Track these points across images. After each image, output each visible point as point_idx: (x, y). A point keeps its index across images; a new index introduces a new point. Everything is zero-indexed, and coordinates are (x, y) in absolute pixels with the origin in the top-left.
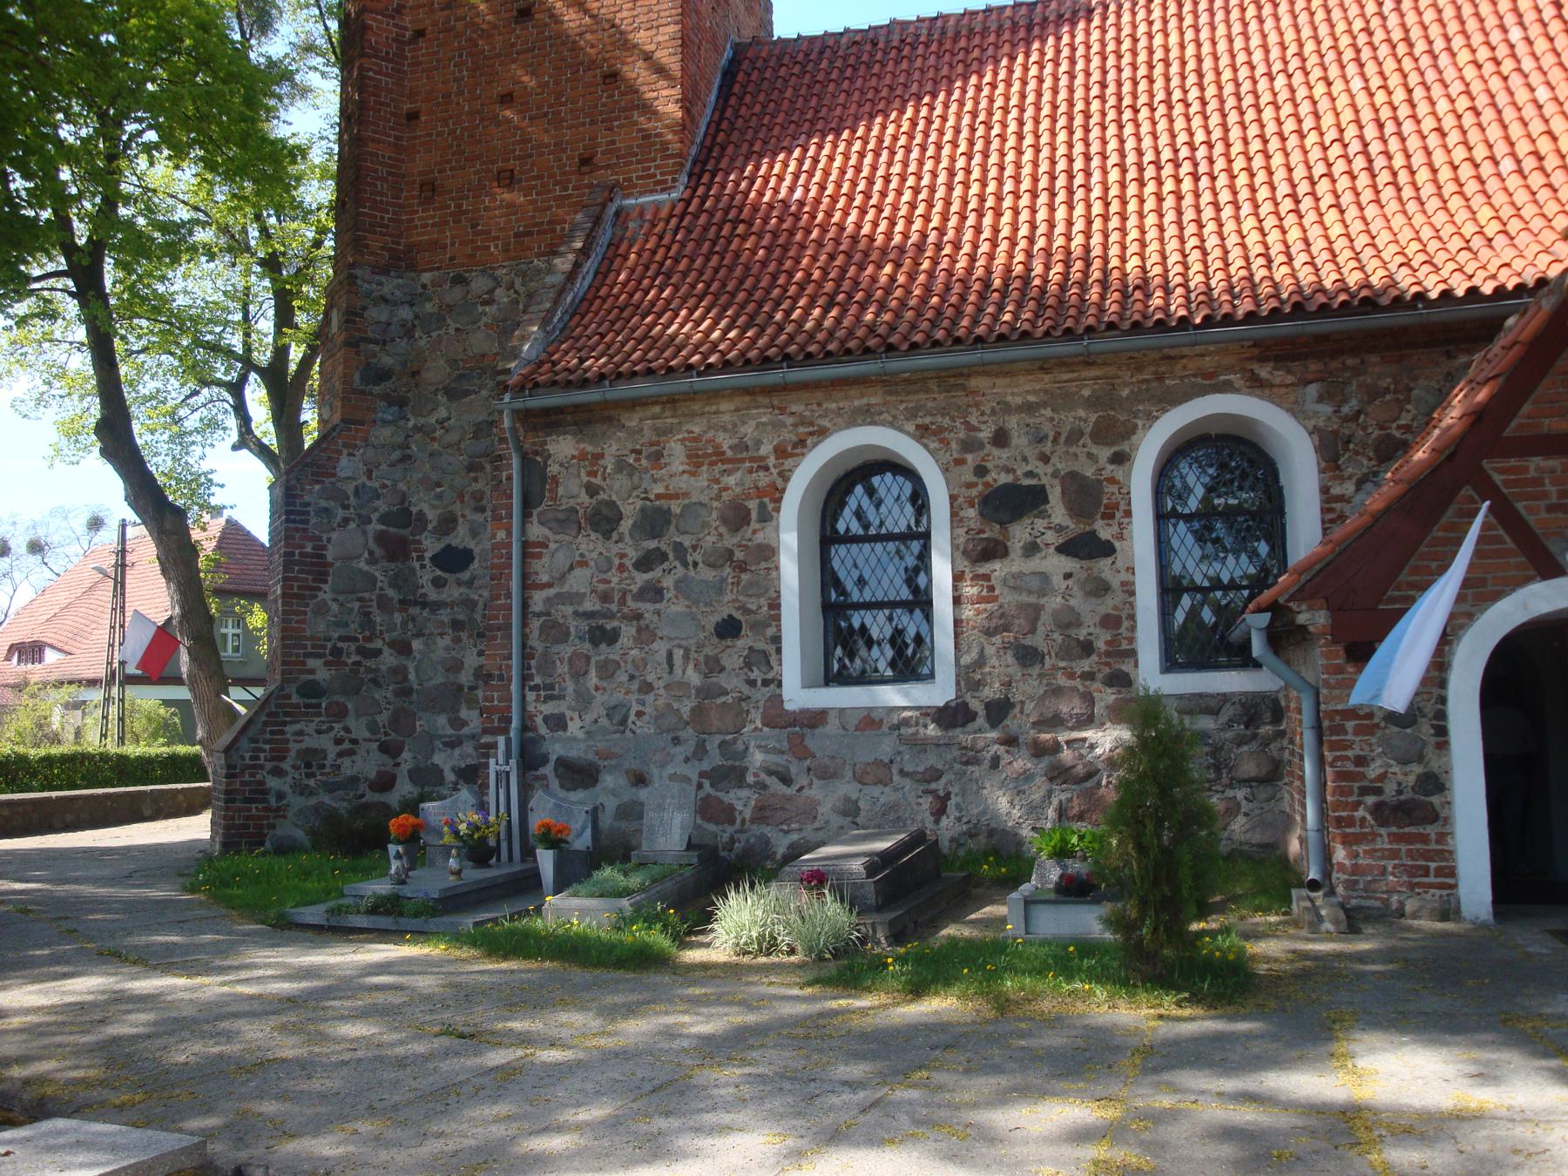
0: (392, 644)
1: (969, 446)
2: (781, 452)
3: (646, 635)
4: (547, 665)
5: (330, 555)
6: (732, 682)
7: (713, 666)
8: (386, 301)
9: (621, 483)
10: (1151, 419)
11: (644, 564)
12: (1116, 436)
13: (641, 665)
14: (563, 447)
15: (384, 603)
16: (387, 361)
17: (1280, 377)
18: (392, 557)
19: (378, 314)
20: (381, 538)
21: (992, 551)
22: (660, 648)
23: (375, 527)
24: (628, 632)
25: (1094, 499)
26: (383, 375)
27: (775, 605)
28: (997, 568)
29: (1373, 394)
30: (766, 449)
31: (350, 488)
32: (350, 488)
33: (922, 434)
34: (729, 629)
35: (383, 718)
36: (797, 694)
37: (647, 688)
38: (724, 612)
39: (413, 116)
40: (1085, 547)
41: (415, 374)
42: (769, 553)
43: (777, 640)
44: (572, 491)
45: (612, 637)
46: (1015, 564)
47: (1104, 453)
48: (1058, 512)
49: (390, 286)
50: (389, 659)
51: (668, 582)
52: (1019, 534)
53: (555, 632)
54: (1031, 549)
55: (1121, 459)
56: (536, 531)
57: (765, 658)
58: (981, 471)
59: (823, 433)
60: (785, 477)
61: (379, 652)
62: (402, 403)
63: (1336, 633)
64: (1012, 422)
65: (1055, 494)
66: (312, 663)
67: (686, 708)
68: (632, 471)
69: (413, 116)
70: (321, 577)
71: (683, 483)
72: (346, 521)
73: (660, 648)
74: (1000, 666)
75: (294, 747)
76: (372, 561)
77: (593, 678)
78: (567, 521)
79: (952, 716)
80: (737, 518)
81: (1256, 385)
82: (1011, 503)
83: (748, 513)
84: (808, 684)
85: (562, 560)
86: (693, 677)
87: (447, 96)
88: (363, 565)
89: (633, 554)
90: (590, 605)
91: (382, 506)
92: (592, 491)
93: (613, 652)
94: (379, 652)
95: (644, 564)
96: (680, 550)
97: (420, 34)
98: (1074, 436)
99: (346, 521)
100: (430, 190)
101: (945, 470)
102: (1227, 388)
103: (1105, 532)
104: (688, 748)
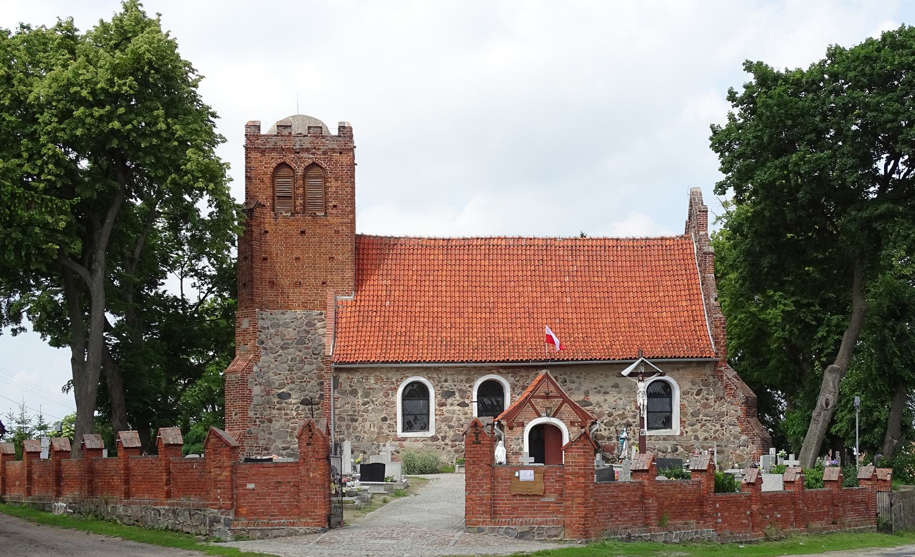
1: (439, 382)
2: (397, 381)
3: (365, 420)
4: (339, 427)
5: (253, 393)
6: (386, 431)
7: (381, 428)
9: (358, 384)
11: (364, 404)
12: (470, 381)
14: (343, 376)
17: (504, 372)
21: (443, 405)
22: (368, 424)
24: (360, 419)
25: (464, 393)
27: (395, 415)
29: (522, 376)
30: (394, 380)
33: (429, 378)
34: (385, 419)
36: (400, 434)
37: (365, 432)
40: (463, 405)
42: (394, 403)
44: (346, 386)
45: (356, 420)
46: (448, 407)
48: (458, 398)
51: (370, 408)
52: (449, 401)
53: (341, 419)
54: (452, 405)
56: (337, 395)
57: (392, 427)
58: (441, 387)
59: (407, 377)
60: (398, 386)
64: (449, 378)
65: (457, 394)
68: (361, 382)
69: (265, 259)
73: (368, 424)
74: (444, 427)
77: (351, 430)
78: (344, 393)
79: (434, 439)
80: (387, 395)
81: (499, 373)
84: (403, 431)
85: (343, 402)
86: (376, 430)
87: (277, 254)
89: (361, 402)
90: (350, 413)
92: (351, 386)
93: (357, 424)
95: (364, 404)
96: (373, 402)
97: (267, 232)
100: (272, 284)
102: (493, 373)
103: (467, 401)
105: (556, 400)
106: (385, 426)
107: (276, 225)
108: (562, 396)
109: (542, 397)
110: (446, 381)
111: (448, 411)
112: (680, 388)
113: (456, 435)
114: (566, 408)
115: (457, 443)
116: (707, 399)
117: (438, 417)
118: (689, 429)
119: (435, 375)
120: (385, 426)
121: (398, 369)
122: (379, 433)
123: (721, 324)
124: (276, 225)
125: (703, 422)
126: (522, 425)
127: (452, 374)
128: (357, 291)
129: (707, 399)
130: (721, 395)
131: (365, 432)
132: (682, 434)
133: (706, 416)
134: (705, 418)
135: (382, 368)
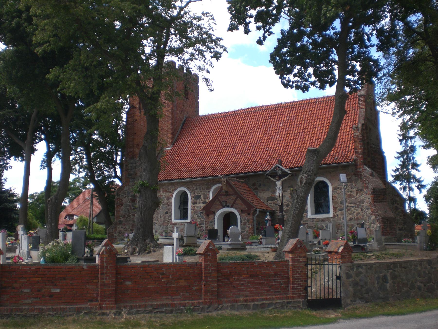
0: (132, 215)
5: (123, 201)
7: (165, 218)
8: (131, 163)
10: (212, 187)
12: (209, 189)
13: (157, 217)
15: (131, 208)
16: (132, 172)
18: (132, 202)
19: (130, 165)
20: (131, 199)
22: (159, 215)
23: (130, 198)
26: (131, 175)
28: (196, 205)
30: (171, 190)
31: (126, 192)
32: (126, 192)
33: (188, 188)
34: (167, 213)
35: (131, 226)
36: (174, 221)
38: (167, 210)
39: (136, 133)
41: (136, 174)
42: (171, 203)
43: (172, 214)
46: (198, 205)
47: (207, 191)
48: (202, 199)
49: (132, 161)
50: (132, 217)
52: (198, 201)
54: (199, 203)
55: (209, 192)
57: (170, 216)
58: (194, 193)
59: (177, 188)
60: (173, 193)
61: (130, 216)
62: (134, 179)
63: (206, 214)
65: (202, 196)
66: (121, 217)
67: (162, 223)
69: (136, 133)
70: (122, 205)
71: (162, 194)
72: (125, 197)
74: (196, 217)
75: (118, 230)
76: (129, 202)
80: (168, 199)
82: (198, 197)
83: (169, 199)
86: (163, 219)
88: (128, 203)
91: (131, 194)
94: (130, 216)
97: (136, 120)
98: (204, 189)
99: (125, 197)
101: (190, 193)
104: (161, 228)
105: (233, 196)
106: (167, 217)
107: (140, 116)
108: (236, 193)
109: (224, 195)
110: (196, 189)
111: (197, 207)
112: (332, 185)
113: (201, 221)
114: (239, 201)
115: (202, 225)
116: (351, 192)
117: (192, 211)
118: (339, 213)
119: (191, 186)
120: (167, 217)
121: (172, 184)
122: (164, 221)
123: (358, 139)
124: (140, 116)
125: (348, 208)
126: (214, 213)
127: (199, 185)
128: (174, 145)
129: (351, 192)
130: (360, 188)
131: (157, 220)
132: (334, 216)
133: (351, 203)
134: (350, 205)
135: (165, 184)
